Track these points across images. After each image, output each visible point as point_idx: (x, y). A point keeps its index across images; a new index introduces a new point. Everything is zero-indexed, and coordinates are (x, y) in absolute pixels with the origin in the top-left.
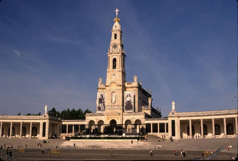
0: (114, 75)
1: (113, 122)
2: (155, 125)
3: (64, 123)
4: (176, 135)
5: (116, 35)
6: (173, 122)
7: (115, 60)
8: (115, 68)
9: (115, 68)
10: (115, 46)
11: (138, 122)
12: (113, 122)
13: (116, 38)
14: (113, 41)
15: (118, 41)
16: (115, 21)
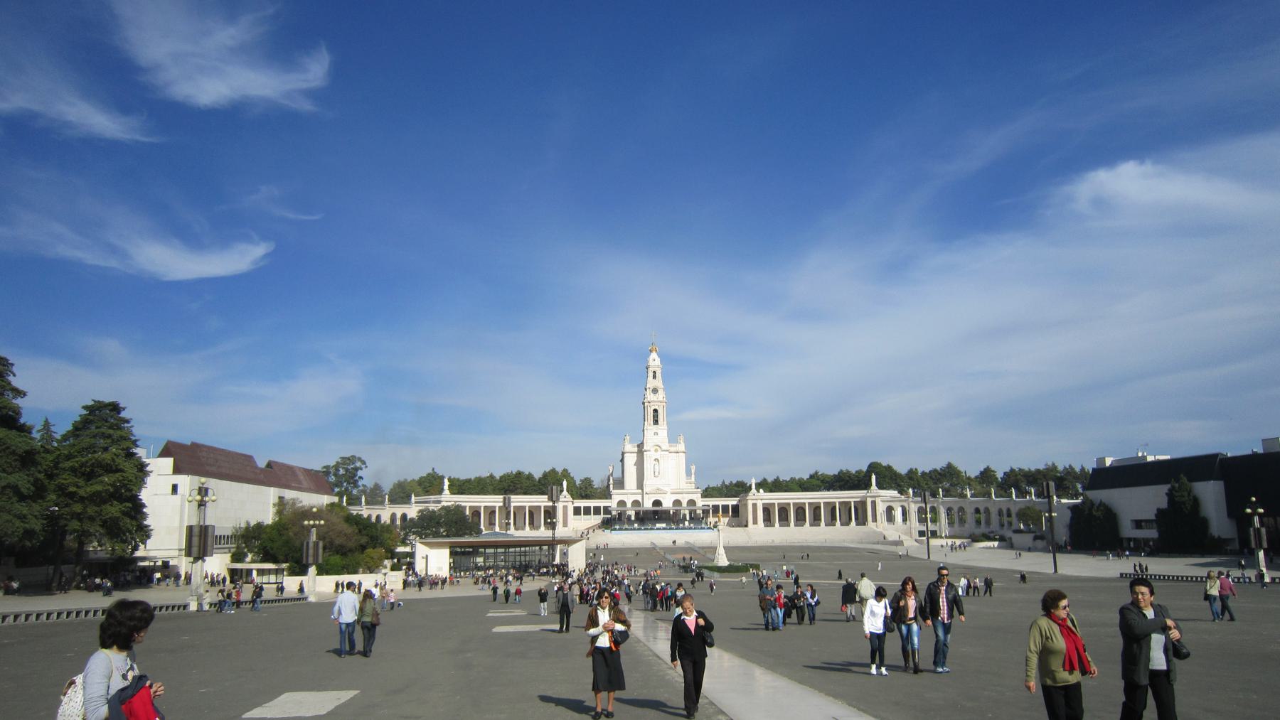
0: (656, 434)
1: (657, 503)
2: (716, 508)
3: (576, 505)
4: (759, 522)
5: (654, 372)
6: (755, 506)
7: (655, 411)
8: (658, 424)
9: (658, 424)
10: (655, 391)
11: (692, 502)
12: (657, 503)
13: (654, 377)
14: (651, 383)
15: (658, 383)
16: (651, 351)
